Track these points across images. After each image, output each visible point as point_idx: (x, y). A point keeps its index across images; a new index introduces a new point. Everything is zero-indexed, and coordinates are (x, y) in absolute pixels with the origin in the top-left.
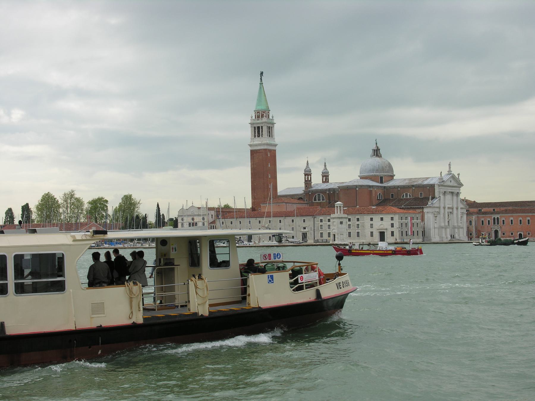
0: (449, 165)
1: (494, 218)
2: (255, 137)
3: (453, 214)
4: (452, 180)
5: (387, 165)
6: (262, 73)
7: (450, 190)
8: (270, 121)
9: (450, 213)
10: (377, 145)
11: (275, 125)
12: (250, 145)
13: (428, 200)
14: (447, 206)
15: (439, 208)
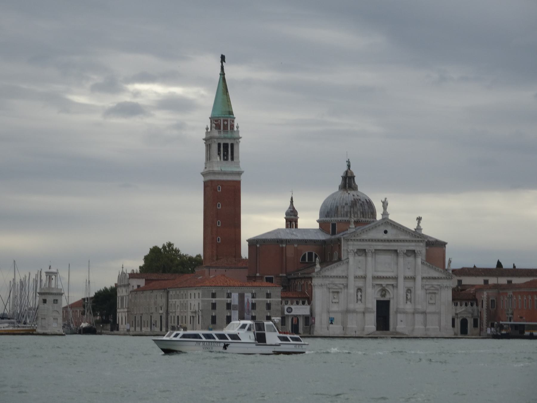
0: (383, 203)
1: (509, 295)
2: (207, 160)
3: (397, 287)
4: (389, 229)
5: (346, 204)
6: (223, 58)
7: (380, 246)
8: (229, 135)
9: (391, 287)
10: (351, 169)
11: (240, 140)
12: (204, 174)
13: (315, 265)
14: (369, 276)
15: (346, 277)
